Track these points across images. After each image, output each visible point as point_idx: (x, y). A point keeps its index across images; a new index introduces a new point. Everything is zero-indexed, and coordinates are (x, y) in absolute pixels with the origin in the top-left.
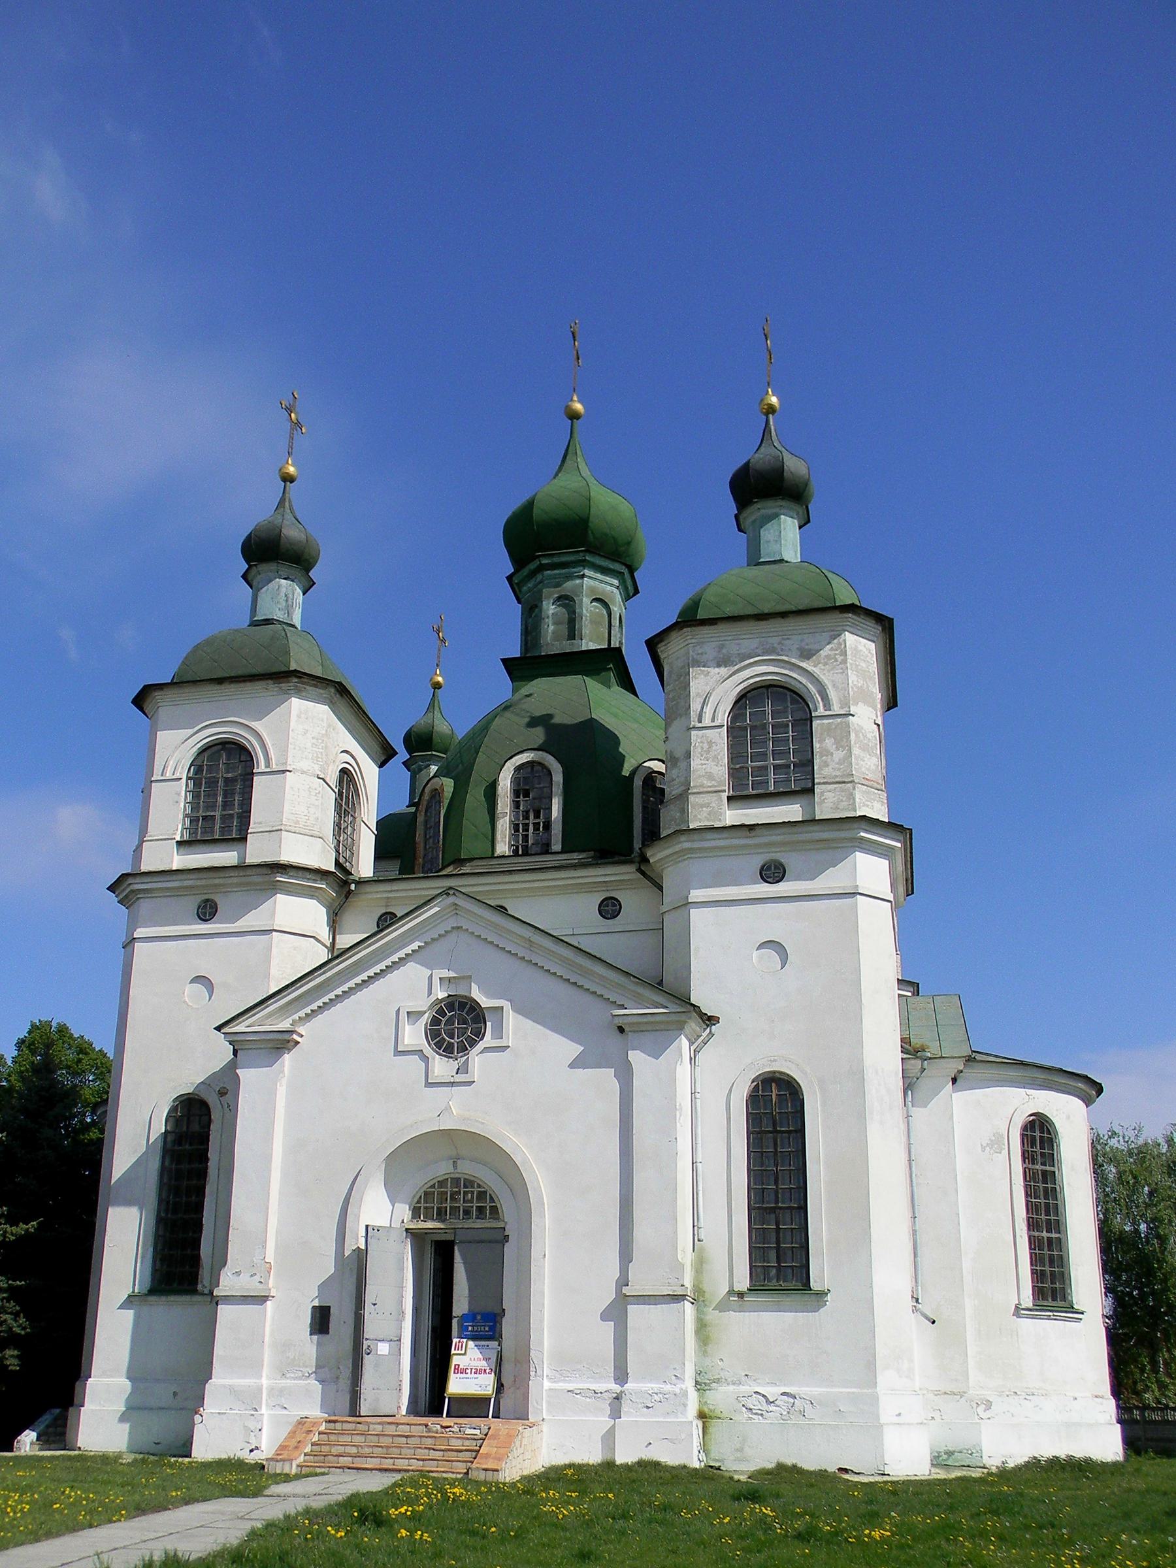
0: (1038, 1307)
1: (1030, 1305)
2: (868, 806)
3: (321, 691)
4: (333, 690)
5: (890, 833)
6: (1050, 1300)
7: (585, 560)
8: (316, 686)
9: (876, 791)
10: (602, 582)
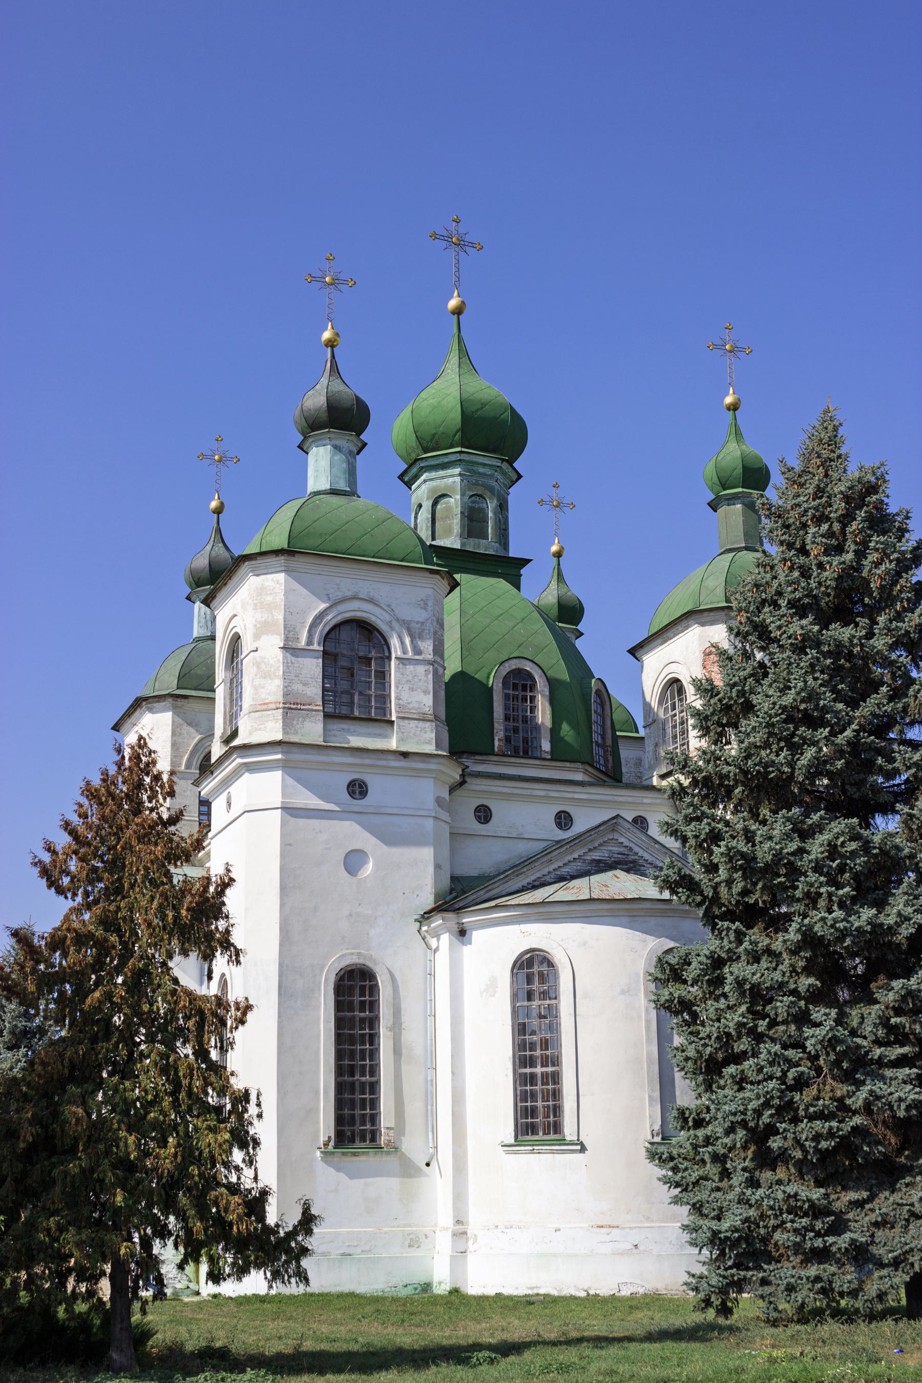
0: (518, 1142)
1: (512, 1141)
2: (260, 729)
3: (164, 703)
4: (170, 700)
5: (270, 749)
6: (541, 1133)
7: (422, 468)
8: (158, 702)
9: (270, 712)
10: (443, 478)
